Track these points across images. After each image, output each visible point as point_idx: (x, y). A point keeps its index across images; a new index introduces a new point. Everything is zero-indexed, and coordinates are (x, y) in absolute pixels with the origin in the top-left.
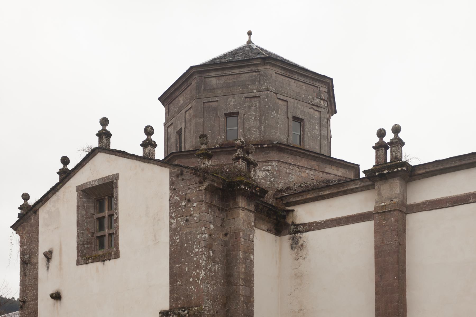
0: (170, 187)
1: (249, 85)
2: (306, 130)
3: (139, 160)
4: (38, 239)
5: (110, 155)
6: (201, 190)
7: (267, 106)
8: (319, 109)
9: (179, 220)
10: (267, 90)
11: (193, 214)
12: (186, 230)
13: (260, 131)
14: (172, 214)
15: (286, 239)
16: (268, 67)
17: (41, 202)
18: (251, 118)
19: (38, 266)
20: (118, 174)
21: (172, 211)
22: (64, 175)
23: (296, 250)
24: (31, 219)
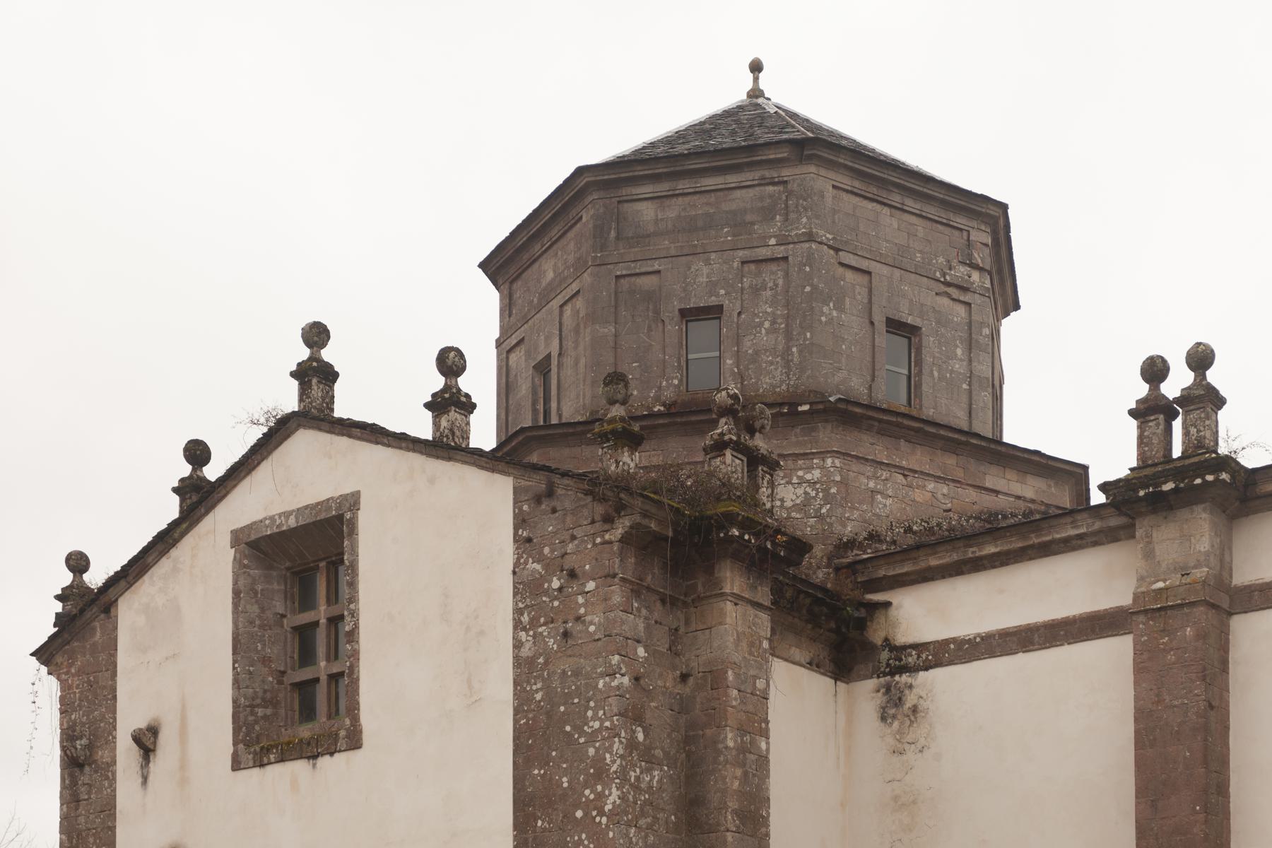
0: (516, 534)
1: (753, 223)
2: (928, 359)
3: (421, 453)
4: (113, 690)
6: (610, 542)
7: (808, 289)
8: (967, 297)
9: (541, 633)
10: (810, 237)
11: (586, 614)
12: (566, 665)
13: (787, 363)
14: (522, 614)
15: (866, 692)
16: (812, 169)
17: (124, 579)
18: (761, 325)
19: (114, 774)
20: (358, 492)
21: (521, 605)
22: (195, 498)
23: (896, 724)
24: (94, 629)
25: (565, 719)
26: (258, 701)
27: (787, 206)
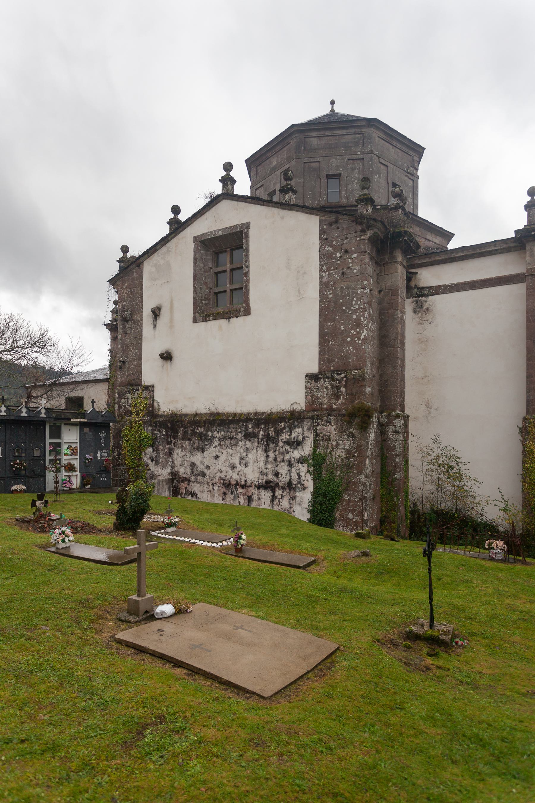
1: (351, 147)
3: (278, 208)
4: (142, 294)
5: (238, 202)
6: (364, 239)
7: (371, 169)
9: (332, 273)
10: (372, 152)
11: (352, 266)
12: (343, 285)
16: (373, 129)
18: (354, 181)
19: (142, 324)
20: (250, 222)
21: (322, 263)
22: (176, 226)
23: (420, 314)
25: (342, 305)
26: (203, 298)
27: (363, 142)
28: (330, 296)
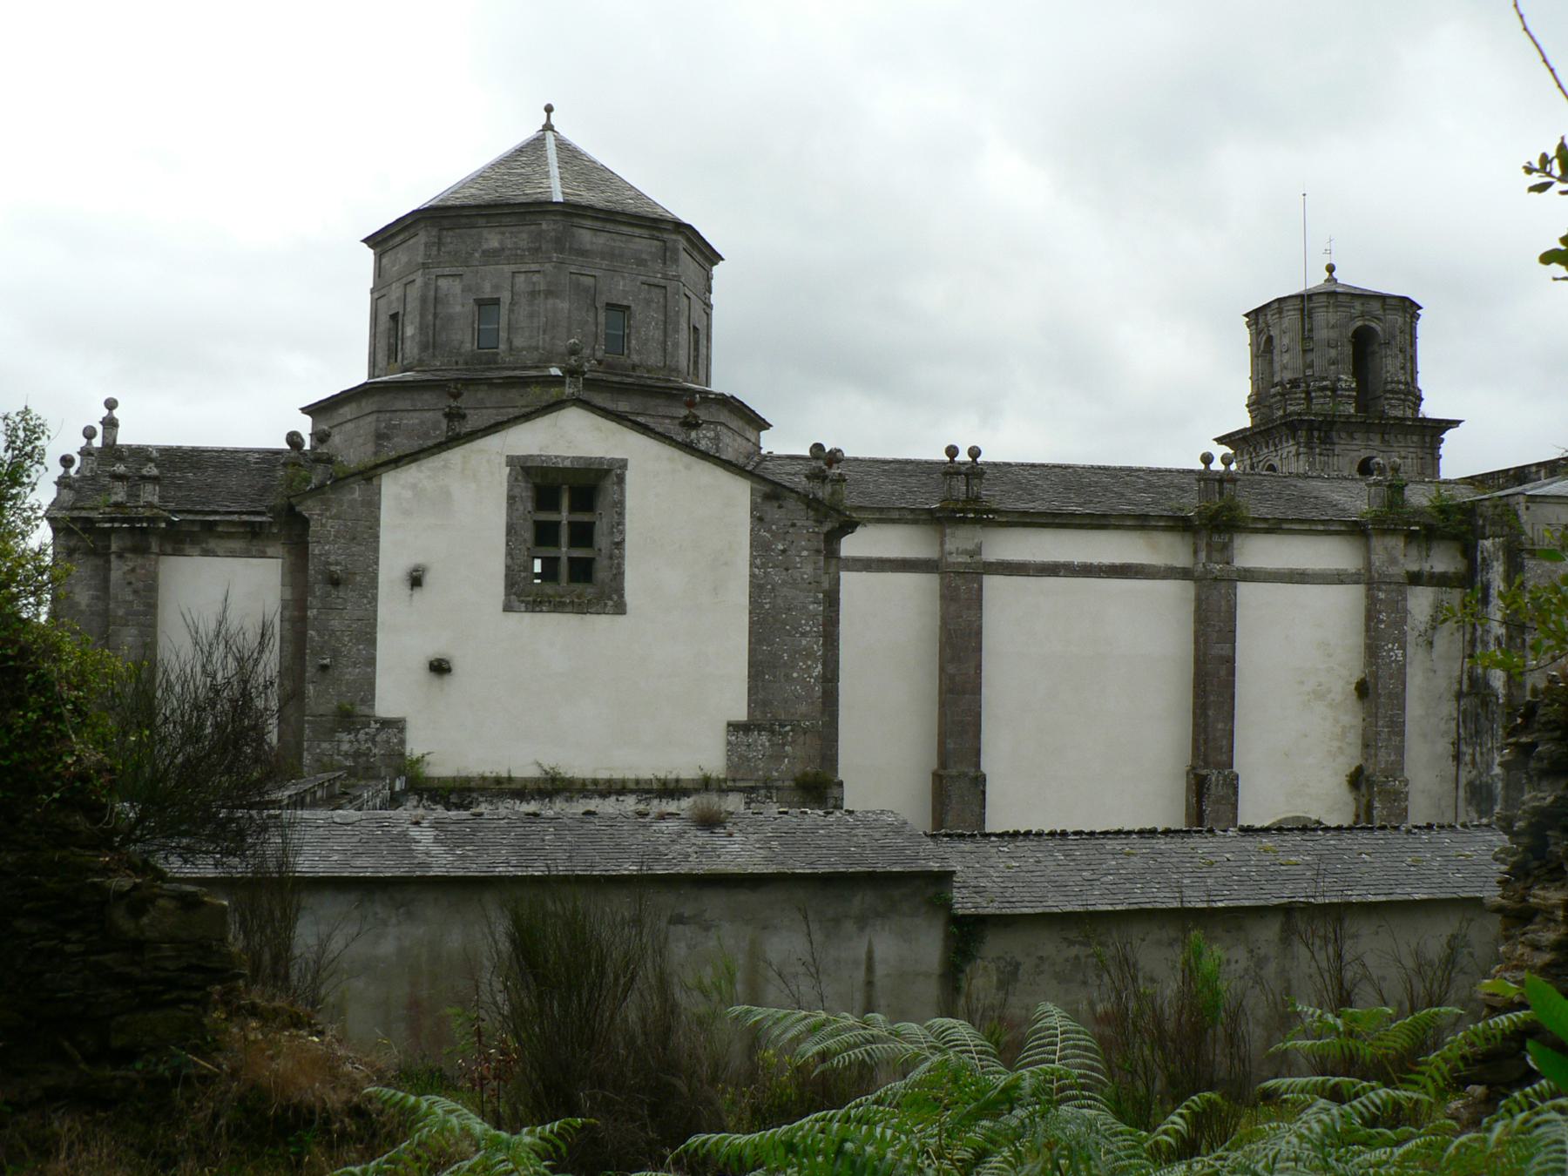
0: (752, 513)
25: (785, 623)
28: (767, 606)
